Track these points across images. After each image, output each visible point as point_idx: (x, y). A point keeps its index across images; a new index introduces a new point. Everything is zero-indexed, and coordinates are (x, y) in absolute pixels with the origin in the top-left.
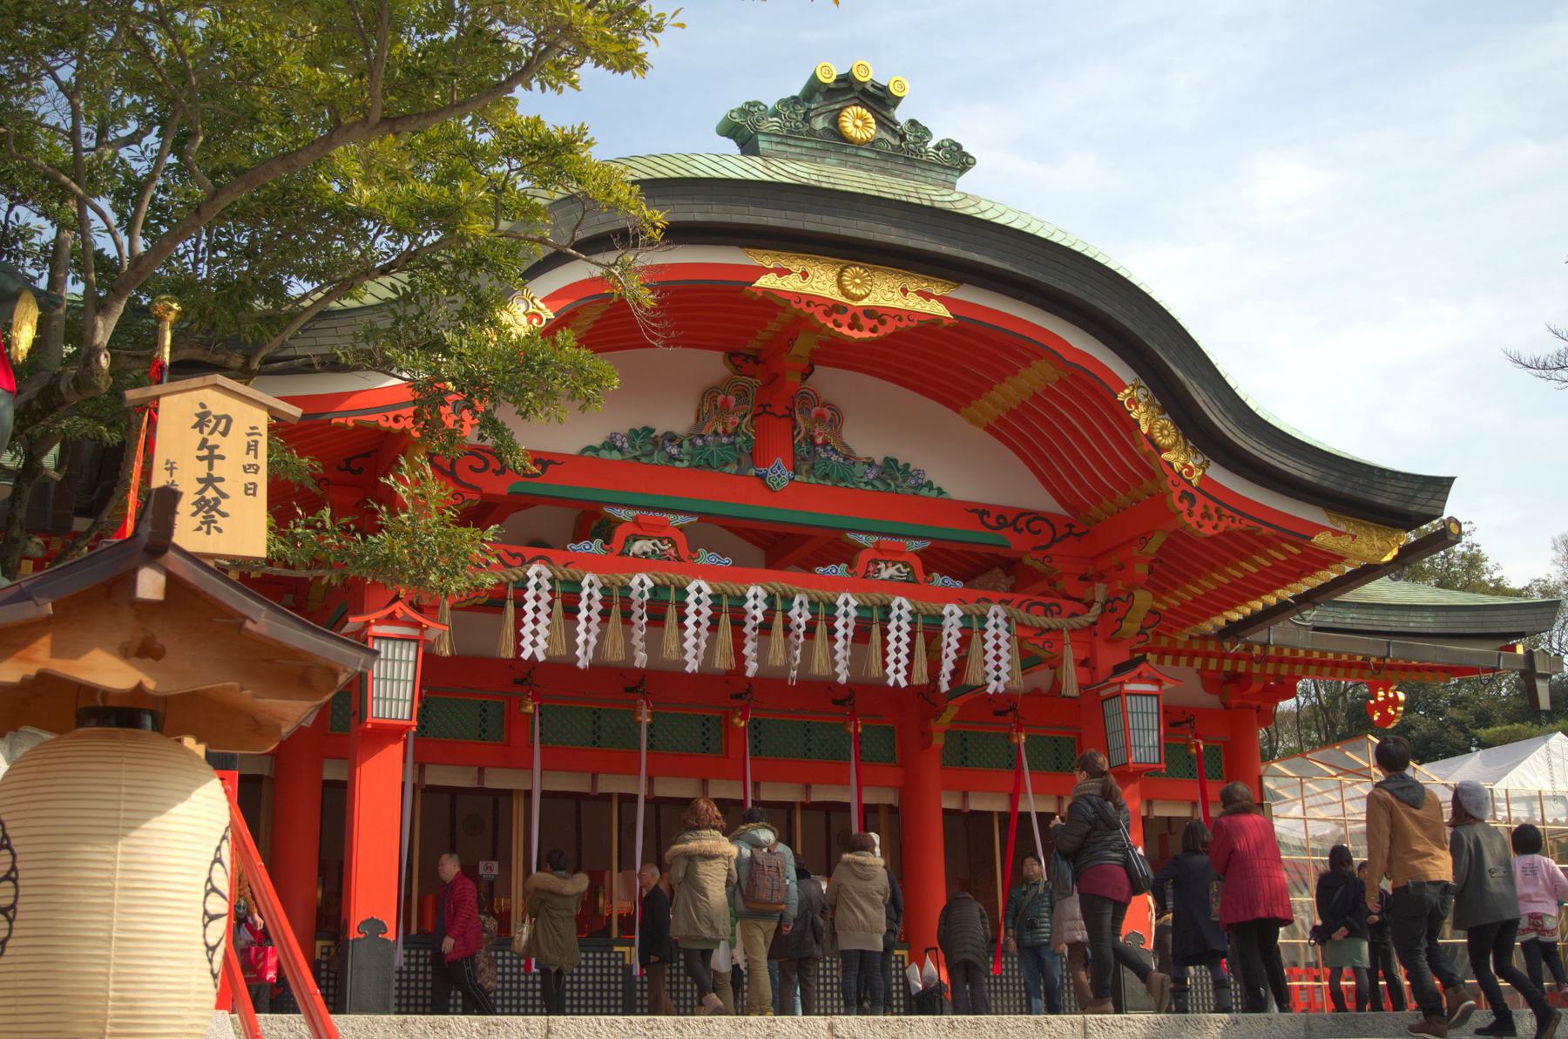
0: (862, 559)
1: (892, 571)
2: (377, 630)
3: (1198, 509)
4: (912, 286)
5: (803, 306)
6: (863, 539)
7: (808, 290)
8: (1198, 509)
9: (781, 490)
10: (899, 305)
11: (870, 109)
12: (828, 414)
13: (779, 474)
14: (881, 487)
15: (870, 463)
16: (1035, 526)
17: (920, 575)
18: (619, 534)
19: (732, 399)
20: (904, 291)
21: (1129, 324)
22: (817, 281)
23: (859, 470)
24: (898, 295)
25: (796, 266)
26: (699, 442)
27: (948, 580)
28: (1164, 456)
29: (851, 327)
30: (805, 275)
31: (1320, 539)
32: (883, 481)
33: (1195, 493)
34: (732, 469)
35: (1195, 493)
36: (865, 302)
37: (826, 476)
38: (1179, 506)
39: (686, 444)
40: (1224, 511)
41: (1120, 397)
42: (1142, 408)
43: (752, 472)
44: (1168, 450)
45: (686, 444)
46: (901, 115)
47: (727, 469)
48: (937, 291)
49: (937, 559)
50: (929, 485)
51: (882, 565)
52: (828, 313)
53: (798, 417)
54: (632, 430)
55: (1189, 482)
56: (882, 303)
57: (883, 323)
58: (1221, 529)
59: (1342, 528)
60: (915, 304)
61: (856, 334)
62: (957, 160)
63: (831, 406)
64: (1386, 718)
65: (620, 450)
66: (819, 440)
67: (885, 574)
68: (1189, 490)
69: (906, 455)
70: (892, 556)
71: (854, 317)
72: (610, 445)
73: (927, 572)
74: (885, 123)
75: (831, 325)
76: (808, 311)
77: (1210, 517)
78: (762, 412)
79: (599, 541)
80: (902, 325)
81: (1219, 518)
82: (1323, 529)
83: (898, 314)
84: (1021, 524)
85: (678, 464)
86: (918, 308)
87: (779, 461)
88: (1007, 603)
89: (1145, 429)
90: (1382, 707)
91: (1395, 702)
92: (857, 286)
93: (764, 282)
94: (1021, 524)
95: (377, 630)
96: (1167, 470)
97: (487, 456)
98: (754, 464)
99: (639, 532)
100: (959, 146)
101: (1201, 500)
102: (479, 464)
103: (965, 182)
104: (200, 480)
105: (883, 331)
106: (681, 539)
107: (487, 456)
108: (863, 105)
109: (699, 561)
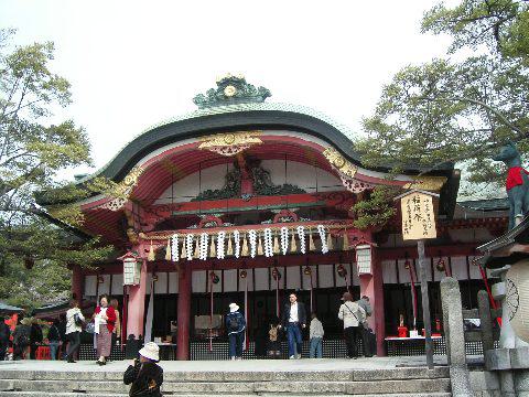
6: (276, 211)
8: (353, 185)
22: (217, 143)
25: (213, 137)
41: (324, 153)
58: (363, 189)
60: (251, 140)
61: (230, 154)
62: (265, 94)
101: (354, 182)
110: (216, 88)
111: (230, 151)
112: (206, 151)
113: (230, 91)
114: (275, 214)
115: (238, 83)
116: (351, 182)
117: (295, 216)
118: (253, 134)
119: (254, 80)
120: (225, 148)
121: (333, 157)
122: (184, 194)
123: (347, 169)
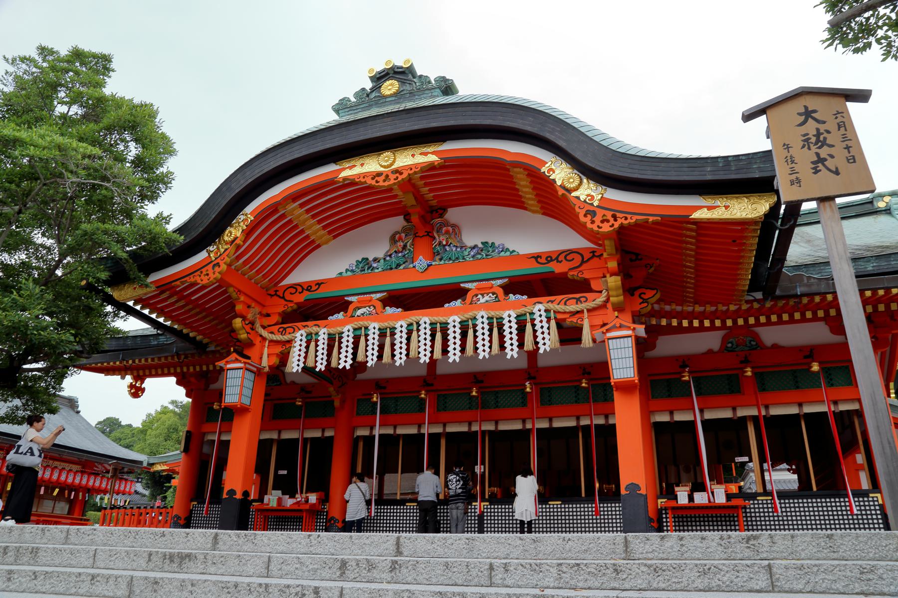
0: (469, 295)
1: (487, 298)
2: (229, 366)
4: (417, 151)
9: (421, 272)
10: (410, 163)
12: (450, 229)
13: (421, 263)
16: (569, 257)
18: (351, 307)
19: (403, 235)
20: (413, 155)
25: (357, 162)
26: (388, 258)
27: (518, 296)
28: (574, 194)
33: (598, 210)
34: (401, 267)
35: (598, 210)
36: (393, 167)
39: (382, 261)
42: (557, 172)
43: (411, 266)
44: (576, 189)
49: (514, 286)
50: (508, 250)
51: (480, 296)
52: (373, 179)
53: (435, 235)
54: (357, 261)
55: (592, 204)
56: (402, 164)
57: (401, 174)
58: (617, 225)
63: (455, 226)
66: (444, 243)
67: (482, 301)
68: (591, 208)
69: (497, 239)
70: (483, 291)
71: (387, 176)
72: (347, 270)
73: (507, 293)
77: (608, 221)
78: (416, 236)
80: (411, 172)
81: (616, 220)
84: (561, 258)
85: (376, 271)
86: (421, 161)
87: (421, 257)
88: (552, 302)
89: (559, 183)
92: (387, 161)
96: (574, 201)
99: (359, 305)
100: (444, 77)
102: (293, 291)
105: (399, 179)
110: (368, 85)
114: (467, 291)
116: (593, 214)
117: (500, 292)
118: (424, 150)
119: (428, 68)
120: (379, 174)
121: (560, 173)
122: (325, 268)
123: (588, 192)
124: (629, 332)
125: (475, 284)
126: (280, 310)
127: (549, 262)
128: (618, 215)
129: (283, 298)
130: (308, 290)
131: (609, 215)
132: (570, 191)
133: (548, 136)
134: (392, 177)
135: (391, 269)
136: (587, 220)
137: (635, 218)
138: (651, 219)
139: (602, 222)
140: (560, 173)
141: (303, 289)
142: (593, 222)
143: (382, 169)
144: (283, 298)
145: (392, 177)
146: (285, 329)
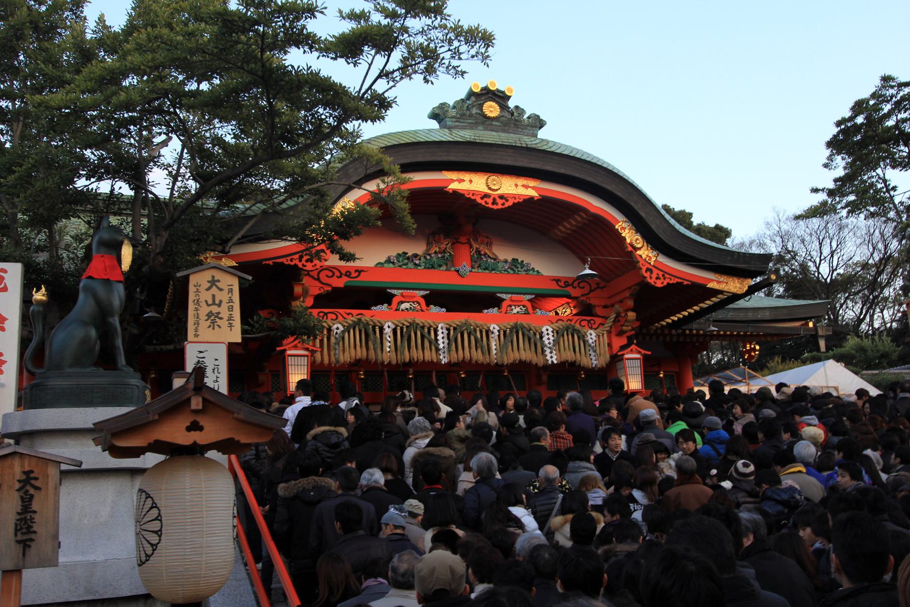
0: (504, 304)
1: (518, 309)
3: (654, 276)
4: (521, 181)
5: (470, 196)
6: (504, 296)
7: (473, 188)
8: (654, 276)
9: (466, 276)
11: (497, 103)
14: (512, 272)
15: (506, 261)
17: (530, 310)
18: (395, 301)
20: (516, 185)
21: (619, 194)
23: (500, 265)
24: (513, 187)
25: (466, 176)
26: (428, 257)
28: (638, 252)
29: (493, 204)
30: (471, 181)
31: (710, 285)
32: (512, 269)
33: (655, 270)
37: (486, 269)
38: (645, 274)
39: (422, 259)
40: (666, 276)
42: (627, 231)
43: (453, 269)
44: (640, 249)
45: (422, 259)
46: (511, 104)
47: (441, 268)
48: (532, 183)
50: (533, 269)
52: (482, 198)
57: (507, 201)
59: (722, 279)
61: (495, 207)
62: (539, 123)
64: (751, 357)
65: (393, 263)
67: (515, 311)
70: (517, 303)
71: (494, 199)
72: (389, 261)
74: (504, 107)
75: (483, 204)
76: (473, 198)
79: (386, 305)
80: (516, 201)
81: (664, 279)
82: (712, 280)
83: (514, 196)
84: (576, 284)
86: (523, 193)
87: (464, 263)
89: (628, 241)
90: (749, 352)
91: (754, 350)
93: (454, 186)
94: (576, 284)
95: (289, 352)
96: (639, 259)
97: (335, 270)
98: (453, 266)
99: (403, 299)
100: (538, 116)
101: (655, 270)
102: (330, 274)
103: (542, 134)
104: (209, 282)
105: (507, 205)
106: (423, 302)
107: (335, 270)
108: (494, 101)
109: (431, 311)
111: (494, 203)
112: (455, 193)
113: (491, 109)
115: (501, 98)
117: (529, 305)
120: (486, 196)
121: (629, 235)
123: (645, 253)
124: (638, 356)
125: (509, 296)
126: (316, 292)
127: (566, 286)
128: (666, 276)
129: (318, 279)
130: (346, 275)
131: (661, 274)
132: (636, 249)
133: (632, 204)
134: (500, 201)
135: (433, 267)
136: (647, 275)
137: (677, 280)
138: (685, 283)
139: (657, 278)
140: (629, 235)
141: (341, 274)
142: (651, 278)
143: (489, 191)
144: (318, 279)
145: (500, 201)
146: (326, 314)
